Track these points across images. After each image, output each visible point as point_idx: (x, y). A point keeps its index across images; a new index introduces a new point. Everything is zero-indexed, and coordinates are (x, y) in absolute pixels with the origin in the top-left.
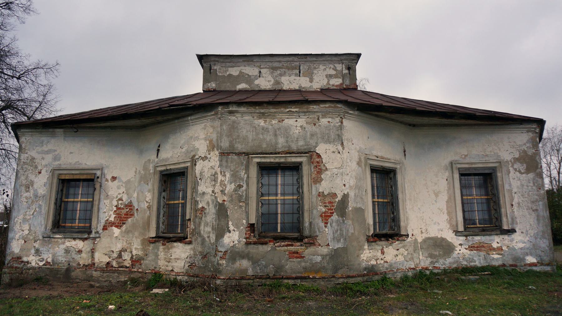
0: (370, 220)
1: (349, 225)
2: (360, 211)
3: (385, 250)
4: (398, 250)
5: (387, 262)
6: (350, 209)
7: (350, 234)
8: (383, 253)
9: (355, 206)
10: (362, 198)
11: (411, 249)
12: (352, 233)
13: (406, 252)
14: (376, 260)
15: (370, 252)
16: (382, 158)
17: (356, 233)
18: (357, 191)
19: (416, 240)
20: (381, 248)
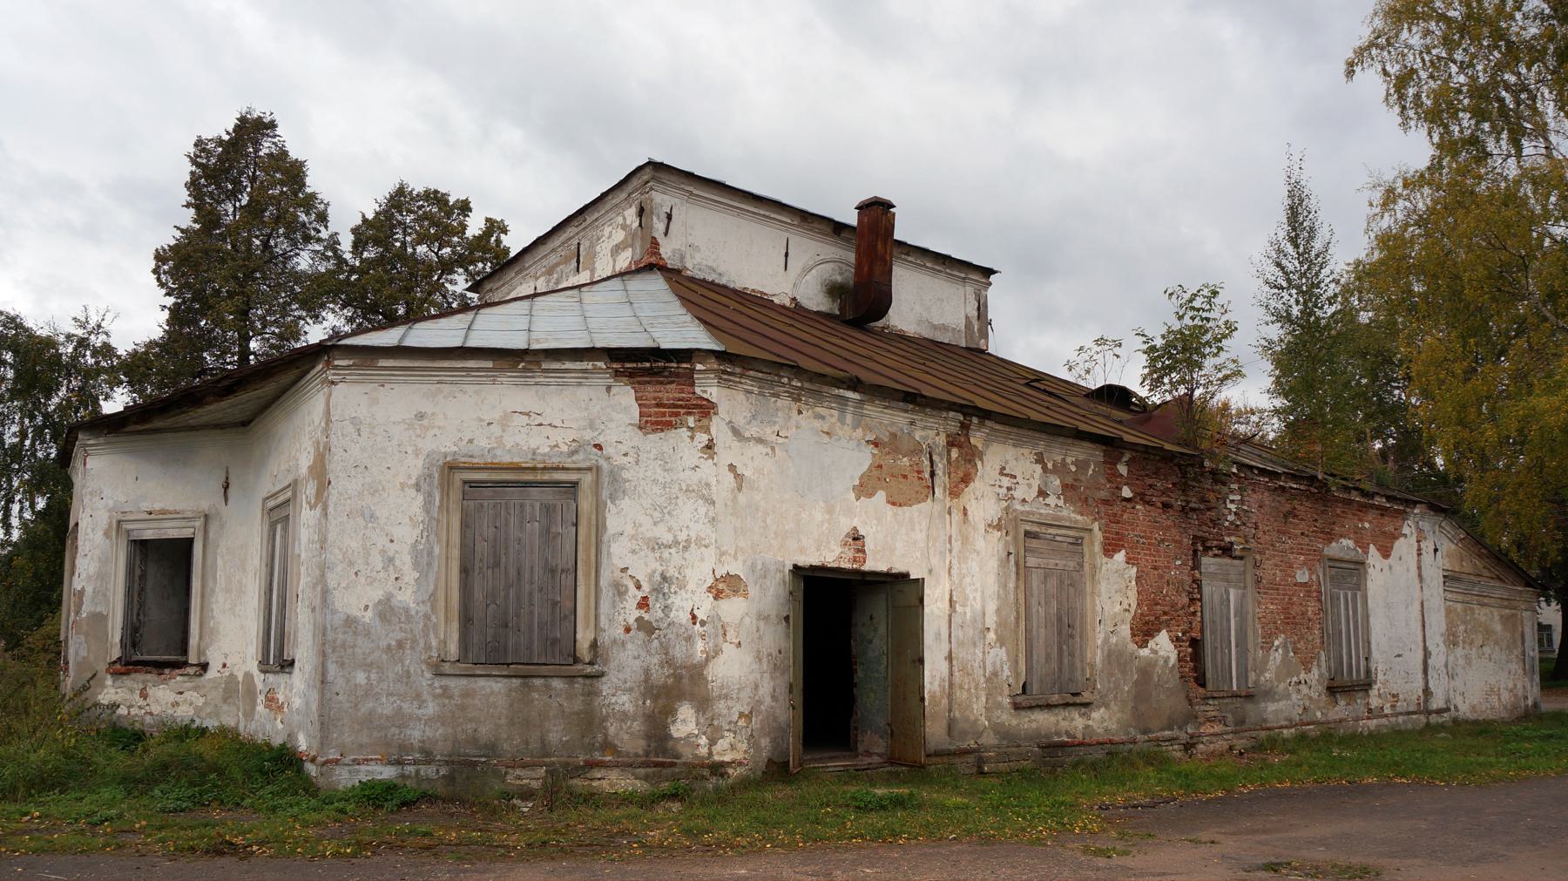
0: (115, 632)
1: (80, 644)
2: (99, 619)
3: (151, 691)
4: (181, 693)
5: (151, 714)
6: (84, 615)
7: (80, 659)
8: (144, 695)
9: (92, 609)
10: (105, 595)
11: (216, 695)
12: (84, 658)
13: (202, 700)
14: (129, 707)
15: (117, 693)
16: (163, 512)
17: (92, 657)
18: (99, 584)
19: (232, 675)
20: (141, 686)
